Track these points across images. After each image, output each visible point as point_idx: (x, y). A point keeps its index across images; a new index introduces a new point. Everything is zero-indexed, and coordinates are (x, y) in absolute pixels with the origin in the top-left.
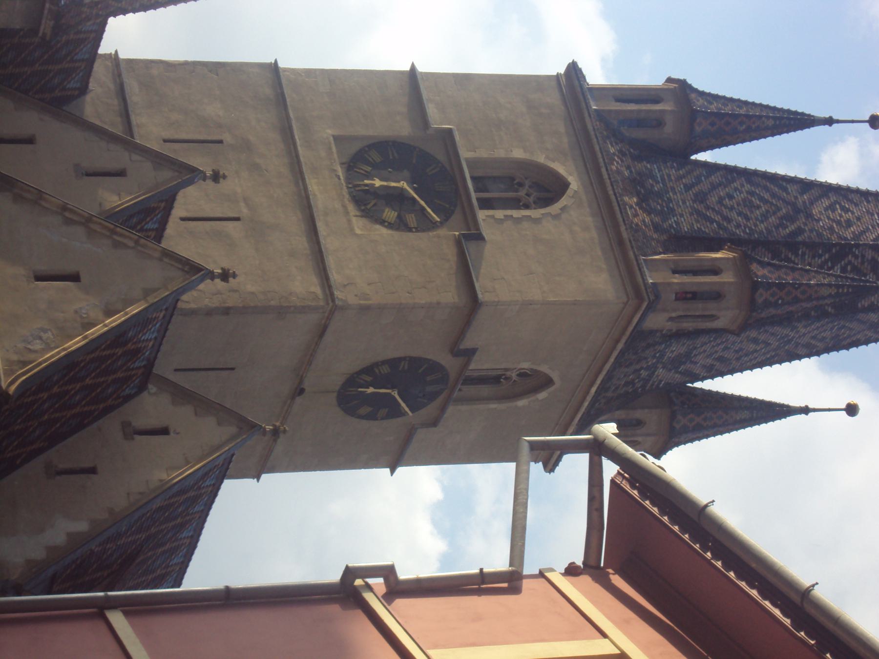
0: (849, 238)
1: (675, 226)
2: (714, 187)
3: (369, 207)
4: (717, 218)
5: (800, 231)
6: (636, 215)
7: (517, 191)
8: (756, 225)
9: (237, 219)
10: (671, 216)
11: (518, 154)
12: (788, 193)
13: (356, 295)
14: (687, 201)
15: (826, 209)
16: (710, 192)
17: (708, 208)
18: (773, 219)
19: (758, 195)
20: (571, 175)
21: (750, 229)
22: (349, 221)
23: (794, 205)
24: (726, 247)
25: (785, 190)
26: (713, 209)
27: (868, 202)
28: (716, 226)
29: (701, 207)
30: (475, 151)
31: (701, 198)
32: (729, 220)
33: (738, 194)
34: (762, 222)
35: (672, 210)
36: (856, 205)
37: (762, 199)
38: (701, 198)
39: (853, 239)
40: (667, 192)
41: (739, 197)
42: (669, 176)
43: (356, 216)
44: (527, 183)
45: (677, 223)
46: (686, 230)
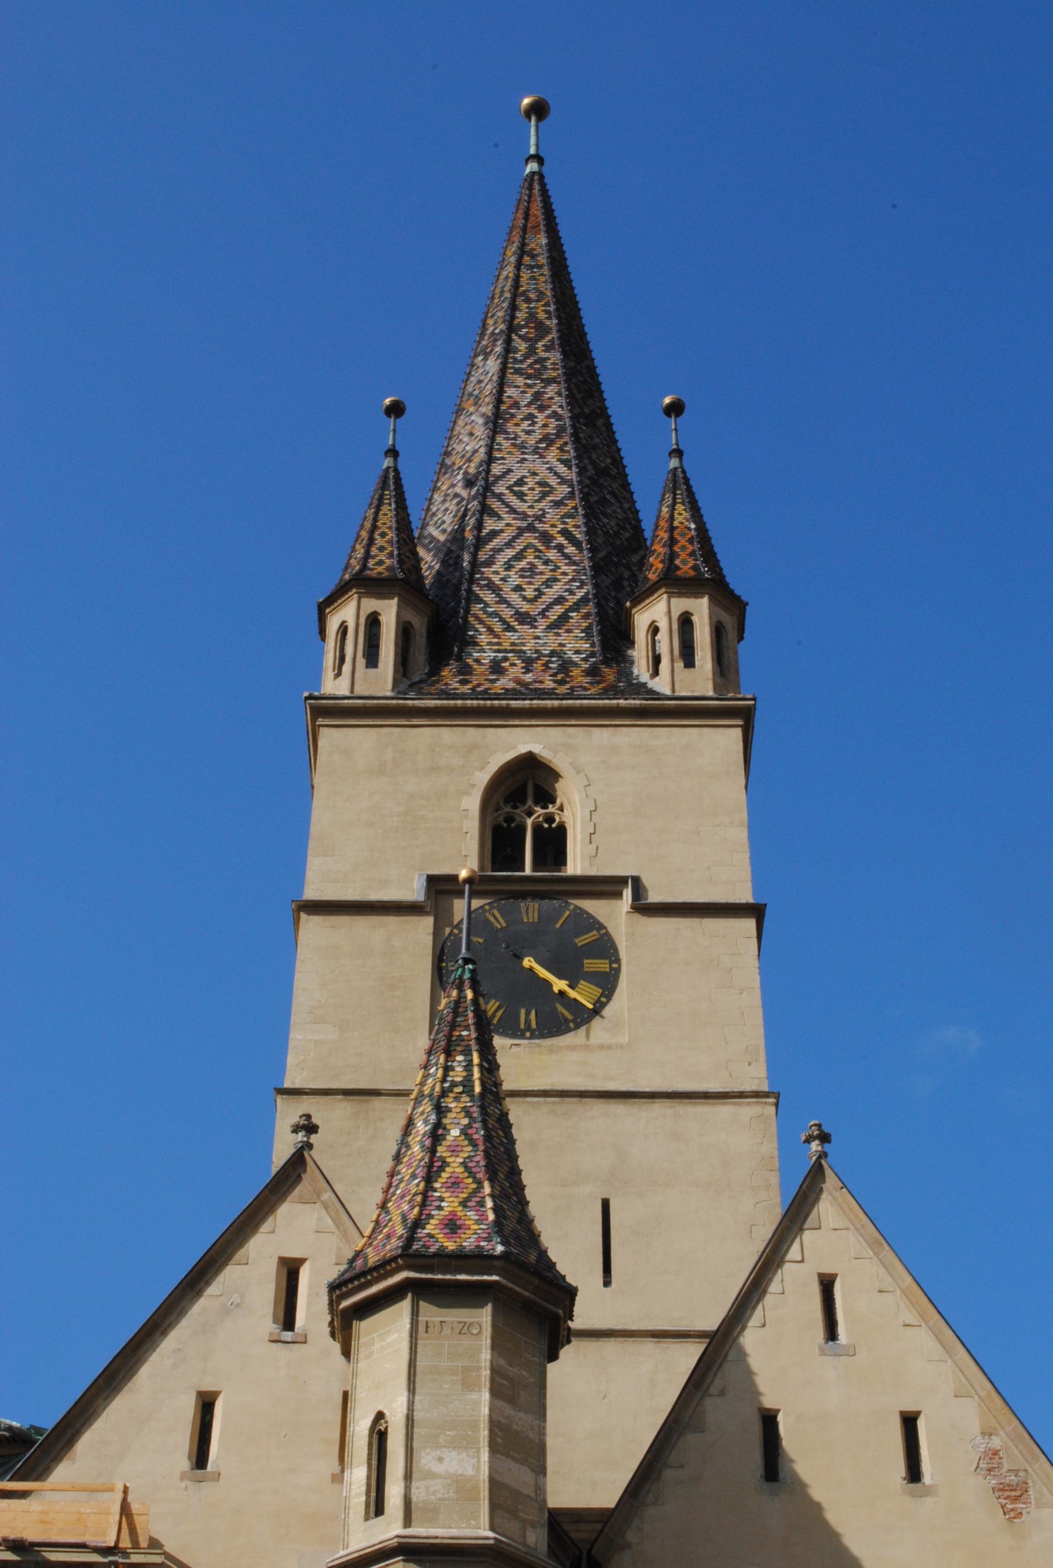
0: (570, 489)
1: (584, 656)
2: (502, 601)
3: (570, 1017)
4: (559, 610)
5: (565, 533)
6: (585, 689)
7: (523, 829)
8: (565, 574)
9: (606, 1205)
10: (566, 656)
11: (473, 803)
12: (502, 531)
13: (750, 1064)
14: (536, 634)
15: (525, 501)
16: (514, 608)
17: (543, 613)
18: (552, 555)
19: (510, 560)
20: (515, 747)
21: (573, 580)
22: (602, 1047)
23: (521, 531)
24: (628, 604)
25: (494, 534)
26: (544, 610)
27: (503, 458)
28: (575, 614)
29: (542, 624)
30: (466, 856)
31: (524, 618)
32: (559, 600)
33: (511, 580)
34: (559, 568)
35: (553, 653)
36: (509, 471)
37: (520, 556)
38: (524, 618)
39: (571, 486)
40: (524, 652)
41: (514, 580)
42: (490, 643)
43: (588, 1036)
44: (508, 809)
45: (577, 652)
46: (588, 645)
